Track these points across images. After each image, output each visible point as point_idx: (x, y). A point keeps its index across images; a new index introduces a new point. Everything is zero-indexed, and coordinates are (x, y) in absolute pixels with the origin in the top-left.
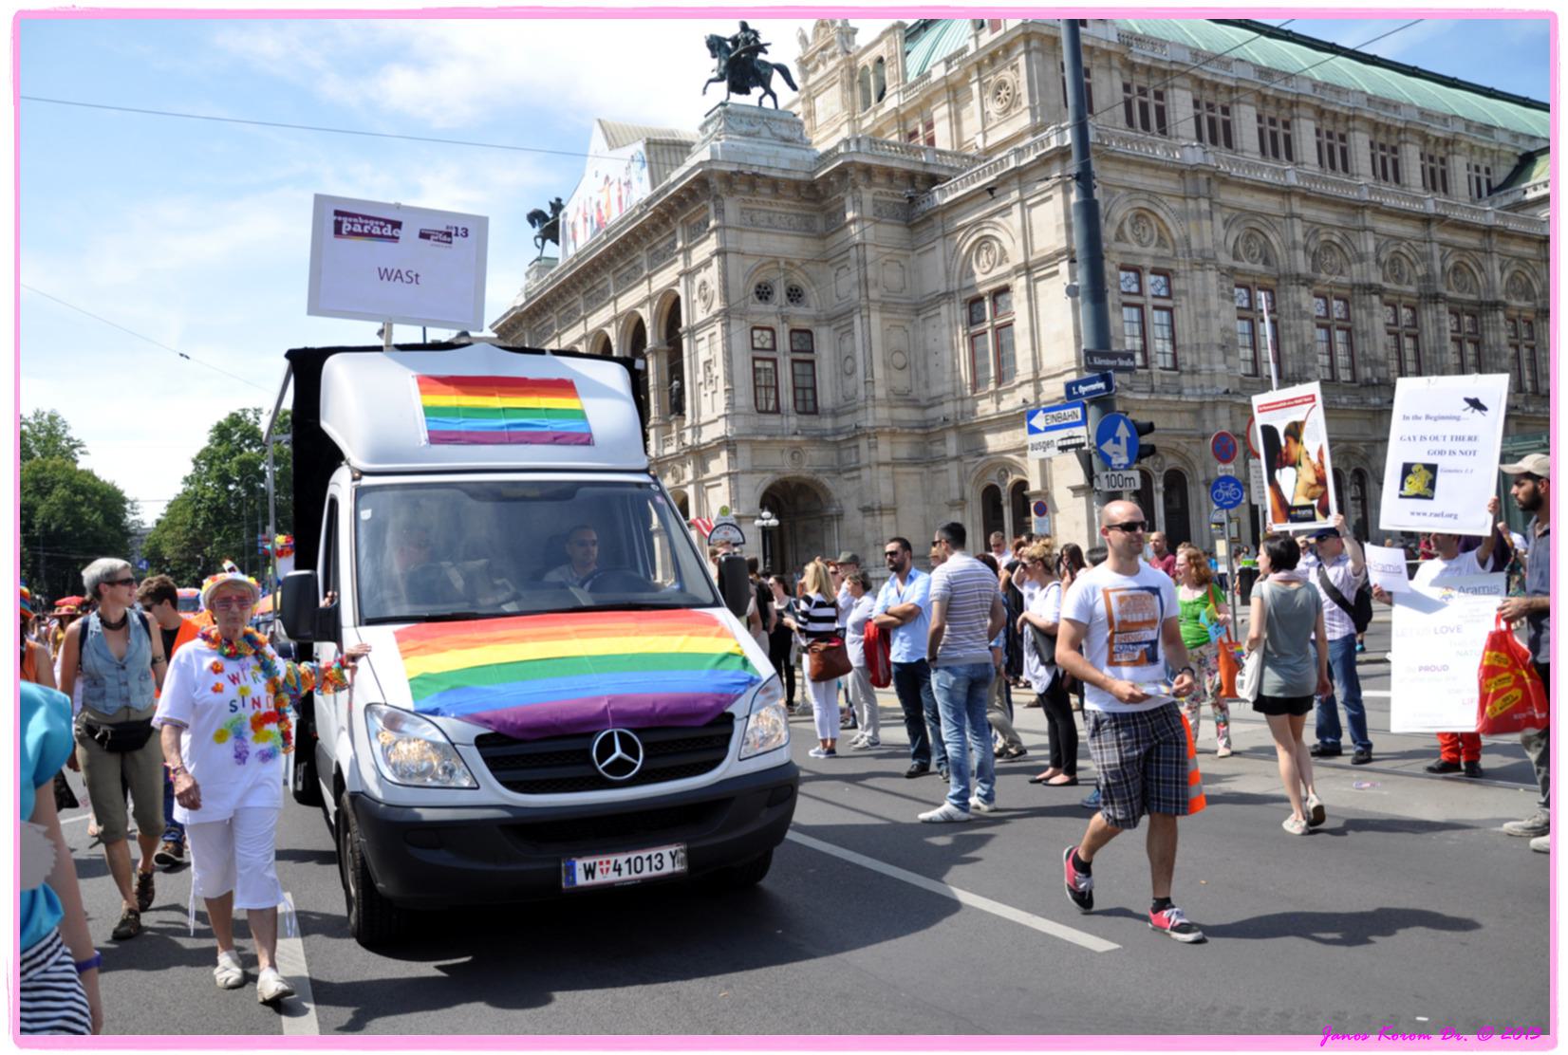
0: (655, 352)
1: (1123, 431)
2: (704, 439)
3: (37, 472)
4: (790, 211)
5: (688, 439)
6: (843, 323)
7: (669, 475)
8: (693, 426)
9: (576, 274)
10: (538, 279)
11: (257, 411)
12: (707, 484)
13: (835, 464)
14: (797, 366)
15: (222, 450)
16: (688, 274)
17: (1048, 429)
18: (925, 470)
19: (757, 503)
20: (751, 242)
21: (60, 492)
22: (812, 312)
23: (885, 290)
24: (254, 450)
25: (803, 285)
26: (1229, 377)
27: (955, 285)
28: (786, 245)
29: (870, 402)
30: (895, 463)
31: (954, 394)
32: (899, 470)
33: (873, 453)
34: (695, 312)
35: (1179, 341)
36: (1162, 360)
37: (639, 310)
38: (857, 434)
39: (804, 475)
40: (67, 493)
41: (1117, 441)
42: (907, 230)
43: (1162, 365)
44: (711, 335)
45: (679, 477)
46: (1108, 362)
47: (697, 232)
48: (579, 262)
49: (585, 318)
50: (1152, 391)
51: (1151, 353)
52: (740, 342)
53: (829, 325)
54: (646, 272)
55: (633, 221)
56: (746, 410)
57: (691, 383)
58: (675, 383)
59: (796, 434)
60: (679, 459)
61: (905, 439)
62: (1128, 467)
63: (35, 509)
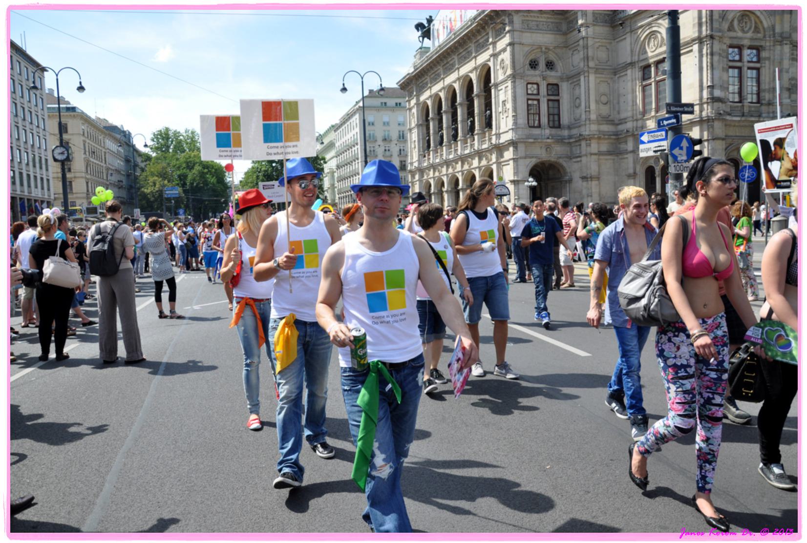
0: (478, 96)
1: (685, 144)
2: (502, 141)
4: (549, 20)
5: (494, 141)
6: (575, 80)
7: (484, 159)
8: (496, 134)
9: (439, 56)
10: (420, 58)
13: (569, 154)
14: (550, 103)
16: (495, 55)
17: (649, 142)
18: (616, 158)
19: (528, 174)
20: (529, 38)
21: (197, 168)
22: (559, 74)
23: (597, 62)
25: (555, 60)
26: (792, 106)
27: (636, 58)
28: (546, 39)
29: (588, 122)
30: (600, 153)
31: (633, 117)
32: (601, 157)
33: (588, 149)
34: (499, 75)
35: (763, 87)
36: (751, 98)
37: (470, 74)
38: (581, 138)
39: (553, 160)
40: (200, 168)
41: (681, 148)
42: (611, 29)
43: (749, 100)
44: (506, 87)
45: (489, 160)
46: (678, 109)
47: (499, 34)
48: (440, 49)
49: (443, 79)
50: (743, 115)
51: (744, 93)
52: (521, 91)
53: (568, 81)
54: (474, 55)
55: (467, 28)
56: (523, 126)
57: (496, 112)
58: (488, 112)
59: (548, 138)
60: (489, 151)
61: (606, 141)
62: (686, 161)
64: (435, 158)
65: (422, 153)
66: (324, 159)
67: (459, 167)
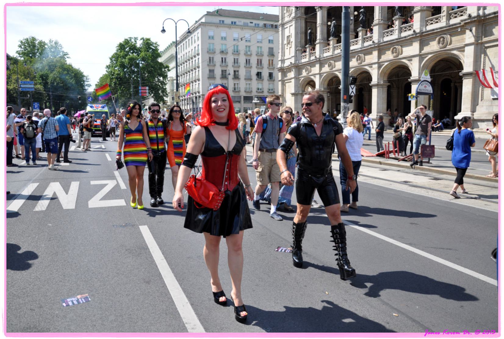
3: (50, 63)
11: (136, 39)
12: (486, 45)
15: (122, 54)
24: (135, 54)
63: (48, 76)
64: (322, 52)
65: (300, 48)
66: (167, 67)
67: (373, 57)
